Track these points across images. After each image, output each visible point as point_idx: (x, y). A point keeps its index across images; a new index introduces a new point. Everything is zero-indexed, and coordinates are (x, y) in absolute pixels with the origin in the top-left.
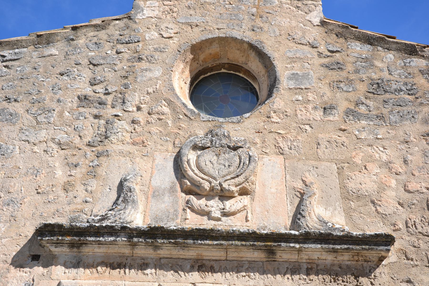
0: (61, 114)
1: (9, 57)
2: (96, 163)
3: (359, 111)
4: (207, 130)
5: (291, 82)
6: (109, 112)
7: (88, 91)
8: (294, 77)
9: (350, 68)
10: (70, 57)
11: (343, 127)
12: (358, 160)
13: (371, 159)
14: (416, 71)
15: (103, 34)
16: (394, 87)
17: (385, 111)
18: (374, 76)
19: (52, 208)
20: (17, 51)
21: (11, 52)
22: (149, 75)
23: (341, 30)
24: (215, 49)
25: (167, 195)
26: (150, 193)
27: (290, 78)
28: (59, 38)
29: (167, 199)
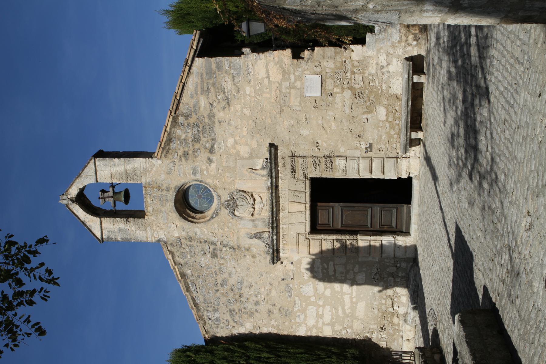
0: (223, 264)
1: (195, 288)
2: (243, 249)
3: (210, 147)
4: (225, 209)
5: (197, 175)
6: (219, 246)
7: (209, 256)
8: (194, 173)
9: (186, 149)
10: (191, 265)
11: (219, 156)
12: (235, 151)
13: (233, 147)
14: (186, 121)
15: (177, 254)
16: (196, 132)
17: (209, 138)
18: (191, 140)
19: (263, 261)
20: (190, 286)
21: (191, 288)
22: (199, 233)
23: (164, 153)
24: (178, 205)
25: (255, 222)
26: (255, 228)
27: (195, 175)
28: (181, 271)
29: (257, 222)
